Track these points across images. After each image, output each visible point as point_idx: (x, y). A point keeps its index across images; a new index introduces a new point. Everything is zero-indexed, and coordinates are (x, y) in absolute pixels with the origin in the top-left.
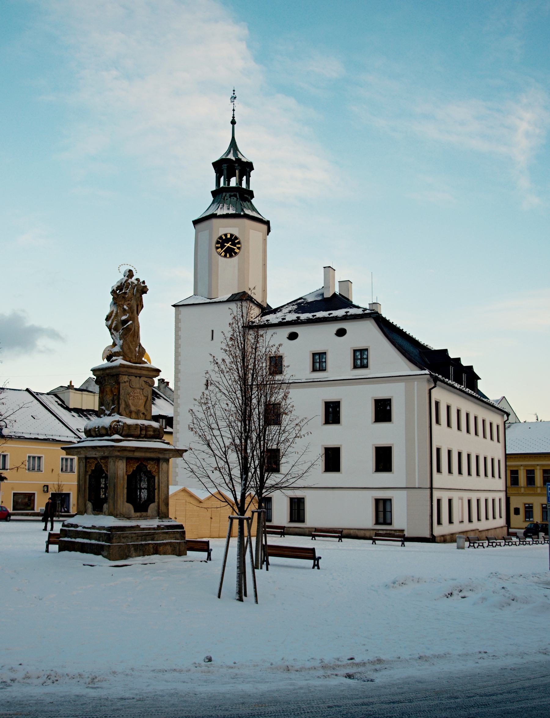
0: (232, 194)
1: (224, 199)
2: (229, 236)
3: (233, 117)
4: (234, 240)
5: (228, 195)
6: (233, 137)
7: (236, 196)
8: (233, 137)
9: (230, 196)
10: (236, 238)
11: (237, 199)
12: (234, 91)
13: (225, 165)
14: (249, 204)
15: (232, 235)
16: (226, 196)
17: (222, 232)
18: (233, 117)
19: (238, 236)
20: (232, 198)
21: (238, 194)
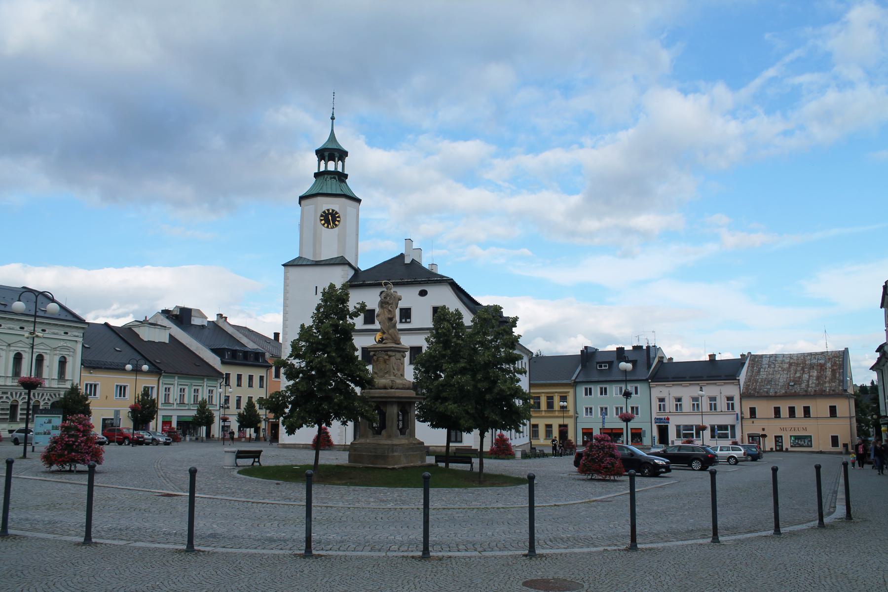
2: (331, 211)
10: (337, 213)
14: (345, 185)
15: (333, 211)
17: (325, 208)
19: (338, 211)
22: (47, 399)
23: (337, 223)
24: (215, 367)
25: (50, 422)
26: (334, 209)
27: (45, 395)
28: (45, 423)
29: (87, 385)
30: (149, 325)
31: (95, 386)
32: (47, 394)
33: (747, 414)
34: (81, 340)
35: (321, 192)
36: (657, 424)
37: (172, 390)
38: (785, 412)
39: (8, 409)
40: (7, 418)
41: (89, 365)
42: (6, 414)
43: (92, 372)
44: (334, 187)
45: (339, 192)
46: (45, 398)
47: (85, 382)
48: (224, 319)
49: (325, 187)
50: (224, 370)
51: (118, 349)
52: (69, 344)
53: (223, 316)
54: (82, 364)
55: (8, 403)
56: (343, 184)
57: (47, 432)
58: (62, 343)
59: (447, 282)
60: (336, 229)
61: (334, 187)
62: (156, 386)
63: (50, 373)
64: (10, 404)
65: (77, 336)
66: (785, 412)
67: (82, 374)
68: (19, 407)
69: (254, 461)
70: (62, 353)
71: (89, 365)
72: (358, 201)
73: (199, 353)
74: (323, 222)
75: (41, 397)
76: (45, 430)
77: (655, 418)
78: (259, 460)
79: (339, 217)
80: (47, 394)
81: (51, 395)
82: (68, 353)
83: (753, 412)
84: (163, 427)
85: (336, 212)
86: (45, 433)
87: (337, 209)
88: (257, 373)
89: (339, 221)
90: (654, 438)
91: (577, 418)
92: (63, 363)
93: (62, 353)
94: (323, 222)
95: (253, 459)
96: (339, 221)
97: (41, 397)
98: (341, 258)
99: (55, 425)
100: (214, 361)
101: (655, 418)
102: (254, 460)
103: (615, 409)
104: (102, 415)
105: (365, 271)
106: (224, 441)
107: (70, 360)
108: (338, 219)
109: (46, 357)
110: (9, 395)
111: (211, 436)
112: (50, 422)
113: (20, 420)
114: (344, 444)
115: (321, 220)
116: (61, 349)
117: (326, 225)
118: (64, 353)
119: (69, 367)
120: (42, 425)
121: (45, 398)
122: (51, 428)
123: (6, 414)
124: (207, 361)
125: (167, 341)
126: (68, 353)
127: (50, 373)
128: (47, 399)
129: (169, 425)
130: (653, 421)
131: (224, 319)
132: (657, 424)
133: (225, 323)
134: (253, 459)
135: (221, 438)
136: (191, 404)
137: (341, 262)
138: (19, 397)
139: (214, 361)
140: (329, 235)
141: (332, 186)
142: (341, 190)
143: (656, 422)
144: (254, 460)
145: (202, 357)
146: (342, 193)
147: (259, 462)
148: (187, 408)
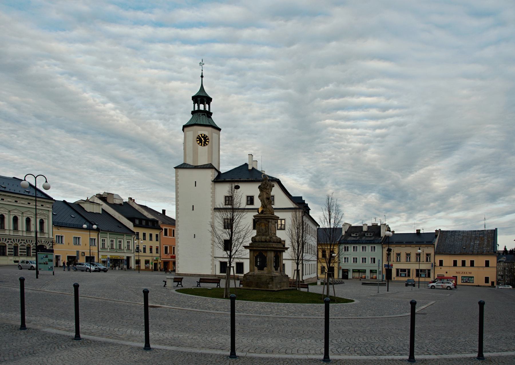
0: (203, 114)
1: (199, 116)
2: (203, 135)
3: (202, 74)
4: (205, 137)
5: (201, 114)
6: (202, 84)
7: (205, 115)
8: (202, 84)
9: (202, 115)
10: (207, 137)
11: (206, 116)
12: (202, 60)
13: (200, 99)
14: (211, 119)
15: (204, 135)
16: (200, 114)
17: (200, 133)
18: (202, 74)
19: (207, 136)
20: (203, 116)
21: (206, 114)
22: (34, 244)
23: (207, 143)
25: (47, 257)
26: (205, 134)
27: (33, 241)
28: (44, 257)
29: (57, 236)
30: (89, 203)
33: (438, 264)
34: (51, 209)
35: (197, 123)
36: (386, 268)
37: (106, 241)
38: (459, 263)
39: (12, 249)
40: (13, 254)
41: (57, 225)
42: (11, 251)
43: (59, 229)
44: (204, 120)
45: (208, 124)
46: (33, 243)
47: (56, 235)
48: (133, 201)
49: (199, 120)
50: (136, 230)
51: (73, 216)
55: (12, 245)
56: (210, 119)
57: (46, 263)
59: (276, 181)
60: (206, 147)
61: (204, 120)
62: (97, 238)
64: (13, 245)
66: (459, 263)
67: (54, 230)
69: (178, 284)
70: (41, 217)
71: (57, 225)
72: (219, 130)
74: (198, 142)
75: (31, 243)
76: (45, 262)
77: (385, 264)
78: (181, 283)
79: (208, 139)
82: (44, 217)
83: (441, 263)
85: (206, 136)
86: (44, 264)
87: (207, 134)
89: (208, 142)
90: (384, 275)
91: (339, 263)
93: (41, 217)
94: (198, 142)
95: (177, 283)
96: (208, 142)
97: (31, 243)
98: (210, 165)
99: (50, 258)
101: (385, 264)
102: (178, 283)
103: (370, 259)
105: (224, 173)
106: (139, 270)
107: (46, 222)
108: (207, 140)
111: (130, 268)
112: (47, 257)
114: (215, 274)
115: (197, 141)
117: (200, 144)
120: (42, 258)
121: (33, 243)
122: (48, 261)
123: (11, 251)
125: (101, 213)
126: (44, 217)
130: (384, 266)
132: (386, 268)
133: (134, 203)
134: (177, 283)
137: (210, 167)
138: (18, 242)
140: (203, 150)
141: (203, 120)
142: (209, 123)
143: (385, 267)
144: (178, 283)
146: (210, 124)
147: (181, 284)
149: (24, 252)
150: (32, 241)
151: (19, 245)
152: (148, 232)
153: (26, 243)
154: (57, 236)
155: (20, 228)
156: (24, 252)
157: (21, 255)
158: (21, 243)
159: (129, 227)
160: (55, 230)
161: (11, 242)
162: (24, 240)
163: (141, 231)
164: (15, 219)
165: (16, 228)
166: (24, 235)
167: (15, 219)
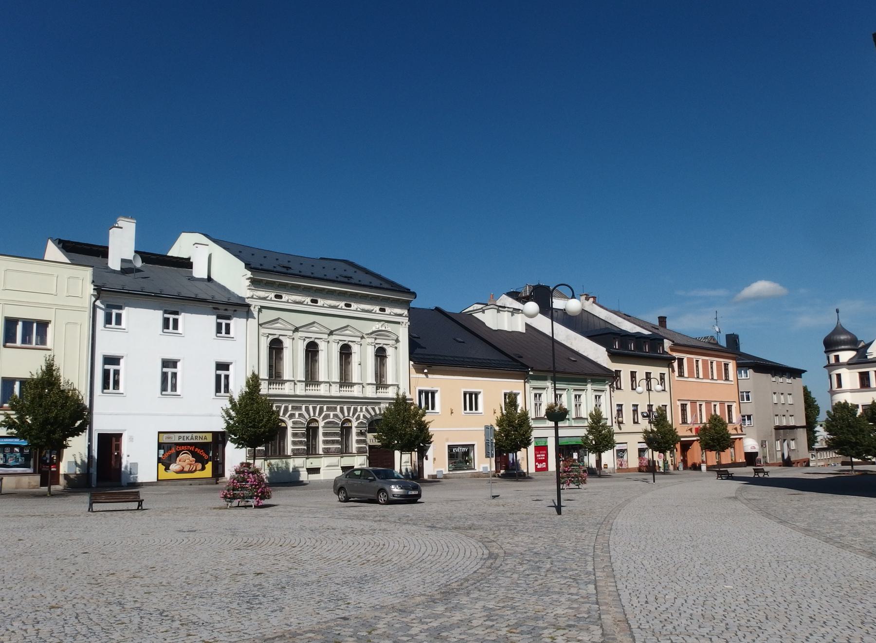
22: (361, 417)
24: (599, 362)
29: (420, 392)
31: (433, 393)
32: (361, 409)
34: (406, 320)
37: (583, 398)
46: (359, 416)
47: (418, 388)
51: (459, 340)
52: (389, 327)
53: (590, 296)
54: (410, 359)
58: (376, 326)
63: (362, 374)
65: (401, 315)
68: (321, 431)
73: (571, 344)
75: (354, 414)
80: (361, 409)
81: (367, 410)
84: (536, 455)
88: (656, 371)
92: (381, 354)
97: (354, 414)
100: (597, 353)
104: (447, 440)
109: (355, 348)
110: (303, 411)
113: (323, 451)
116: (377, 335)
118: (381, 342)
119: (390, 362)
121: (359, 416)
124: (584, 354)
127: (362, 374)
128: (361, 417)
129: (545, 452)
131: (591, 300)
135: (616, 468)
136: (574, 419)
139: (597, 353)
145: (575, 349)
148: (567, 425)
149: (333, 442)
150: (355, 410)
151: (321, 424)
152: (641, 370)
153: (341, 416)
154: (420, 392)
155: (322, 376)
156: (333, 442)
157: (327, 453)
158: (327, 416)
159: (595, 360)
160: (415, 376)
161: (300, 415)
162: (335, 409)
163: (625, 369)
164: (312, 350)
165: (311, 378)
166: (298, 393)
167: (312, 350)
